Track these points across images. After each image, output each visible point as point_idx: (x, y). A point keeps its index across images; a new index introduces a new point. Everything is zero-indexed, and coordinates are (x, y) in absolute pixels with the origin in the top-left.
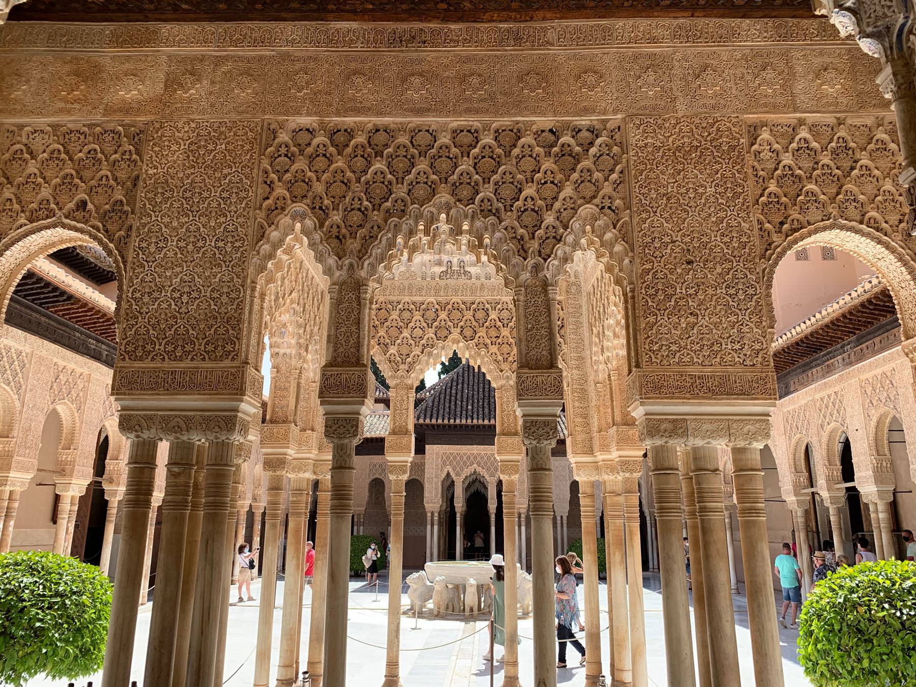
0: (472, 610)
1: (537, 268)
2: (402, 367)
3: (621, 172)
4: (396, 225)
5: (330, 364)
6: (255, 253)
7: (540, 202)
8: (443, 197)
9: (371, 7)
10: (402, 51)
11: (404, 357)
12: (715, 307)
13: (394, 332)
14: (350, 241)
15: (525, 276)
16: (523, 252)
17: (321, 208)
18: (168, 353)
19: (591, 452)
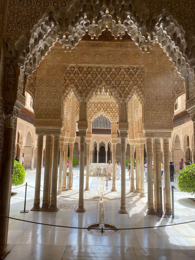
0: (102, 174)
1: (124, 100)
3: (143, 78)
5: (80, 120)
7: (125, 85)
8: (104, 83)
9: (88, 38)
10: (94, 48)
11: (90, 115)
12: (161, 110)
14: (83, 93)
15: (121, 102)
16: (121, 96)
17: (77, 86)
18: (45, 117)
19: (133, 138)
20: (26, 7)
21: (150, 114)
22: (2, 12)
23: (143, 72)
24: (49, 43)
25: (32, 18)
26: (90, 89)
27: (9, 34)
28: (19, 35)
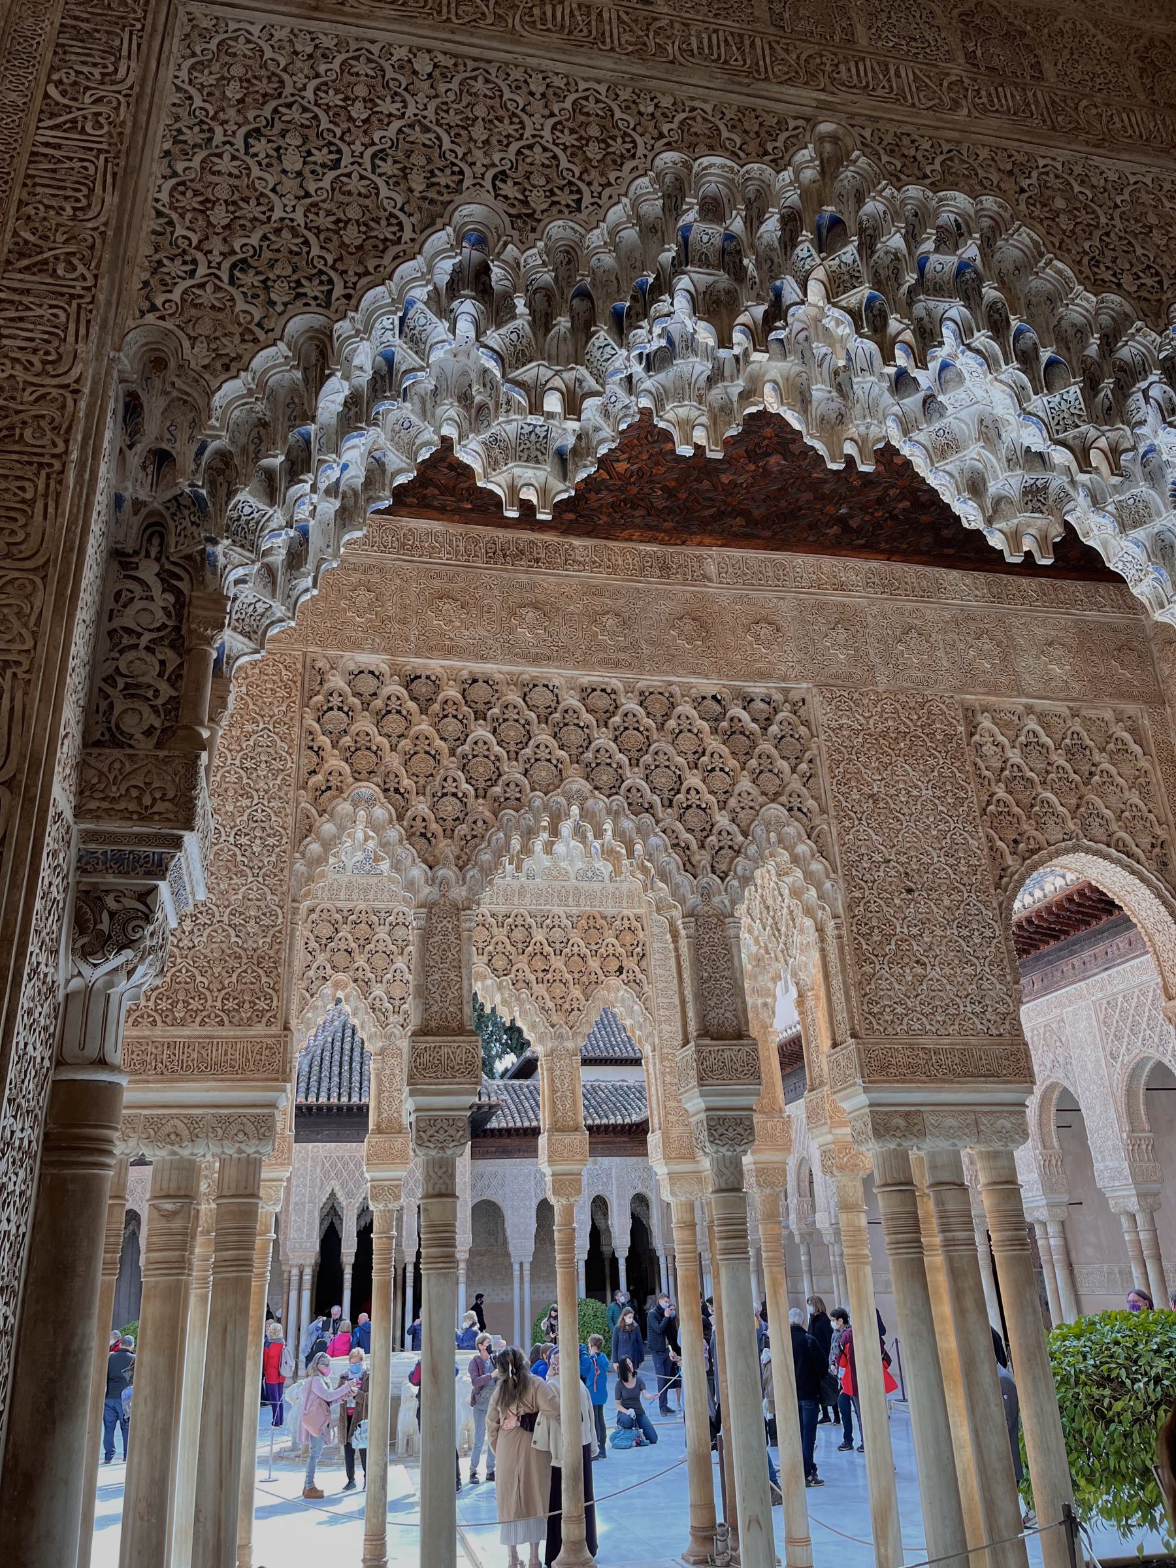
2: (393, 1019)
4: (509, 820)
5: (423, 1031)
6: (297, 855)
10: (506, 570)
11: (397, 1003)
12: (946, 955)
13: (380, 961)
15: (693, 899)
16: (689, 866)
17: (397, 791)
20: (299, 174)
21: (884, 985)
22: (114, 174)
23: (806, 723)
24: (397, 445)
25: (343, 245)
26: (488, 814)
27: (169, 324)
28: (243, 341)
